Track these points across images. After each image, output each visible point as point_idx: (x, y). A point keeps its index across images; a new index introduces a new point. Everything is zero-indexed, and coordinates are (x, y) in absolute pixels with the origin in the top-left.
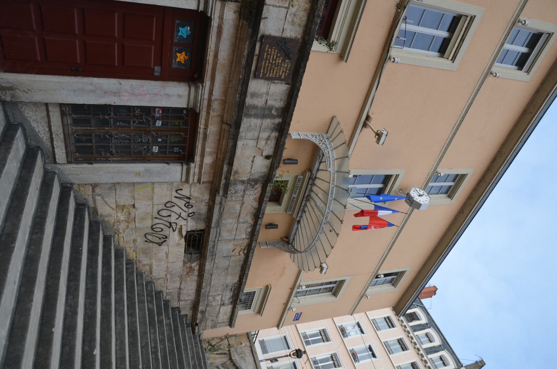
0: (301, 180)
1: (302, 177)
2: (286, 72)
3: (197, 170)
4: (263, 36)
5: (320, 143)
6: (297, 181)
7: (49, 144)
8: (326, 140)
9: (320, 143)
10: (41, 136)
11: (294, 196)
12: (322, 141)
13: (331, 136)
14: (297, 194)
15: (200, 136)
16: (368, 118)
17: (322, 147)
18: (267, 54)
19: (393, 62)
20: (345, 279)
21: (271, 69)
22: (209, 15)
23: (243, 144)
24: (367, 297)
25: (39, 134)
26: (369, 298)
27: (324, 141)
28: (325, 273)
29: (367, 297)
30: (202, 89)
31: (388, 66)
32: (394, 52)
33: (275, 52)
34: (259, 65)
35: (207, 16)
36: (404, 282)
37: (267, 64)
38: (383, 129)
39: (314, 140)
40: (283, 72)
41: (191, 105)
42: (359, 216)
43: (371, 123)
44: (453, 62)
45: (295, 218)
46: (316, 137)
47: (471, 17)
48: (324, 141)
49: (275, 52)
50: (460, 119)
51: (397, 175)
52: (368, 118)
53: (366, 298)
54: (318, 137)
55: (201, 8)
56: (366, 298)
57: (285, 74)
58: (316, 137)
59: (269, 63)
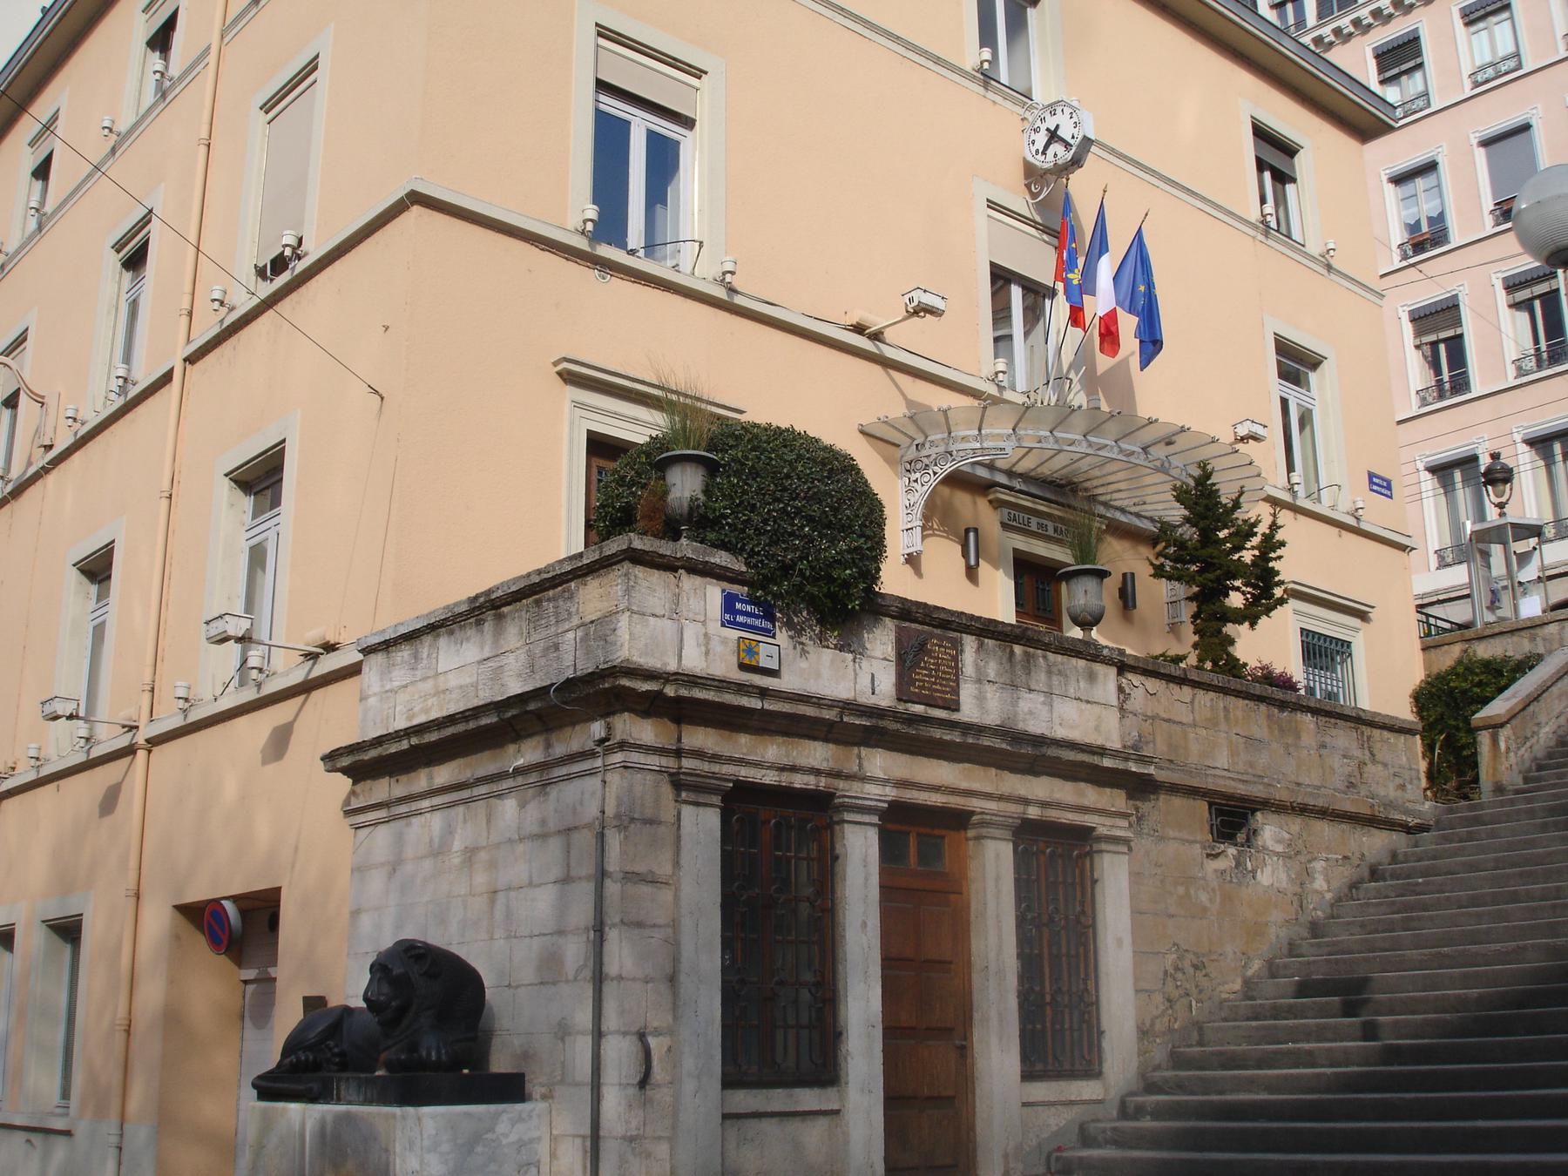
0: (1013, 512)
1: (1006, 511)
2: (945, 647)
3: (1108, 821)
4: (899, 700)
5: (935, 473)
6: (1014, 524)
7: (1076, 1109)
8: (924, 452)
9: (935, 473)
10: (1064, 1122)
11: (1051, 532)
12: (927, 465)
13: (911, 437)
14: (1045, 522)
15: (785, 779)
16: (859, 329)
17: (948, 468)
18: (923, 688)
19: (732, 273)
20: (1273, 336)
21: (943, 679)
22: (886, 805)
23: (1061, 724)
24: (1328, 251)
25: (1062, 1125)
26: (1331, 246)
27: (925, 460)
28: (1265, 426)
29: (1328, 251)
30: (987, 814)
31: (753, 289)
32: (700, 271)
33: (919, 674)
34: (940, 703)
35: (888, 808)
36: (1289, 118)
37: (938, 687)
38: (907, 297)
39: (926, 488)
40: (946, 653)
41: (1007, 834)
42: (1113, 329)
43: (876, 322)
44: (706, 73)
45: (1106, 522)
46: (916, 481)
47: (600, 34)
48: (926, 461)
49: (919, 674)
50: (840, 19)
51: (988, 206)
52: (859, 329)
53: (1332, 252)
54: (914, 476)
55: (875, 819)
56: (1332, 252)
57: (949, 648)
58: (916, 481)
59: (935, 683)
